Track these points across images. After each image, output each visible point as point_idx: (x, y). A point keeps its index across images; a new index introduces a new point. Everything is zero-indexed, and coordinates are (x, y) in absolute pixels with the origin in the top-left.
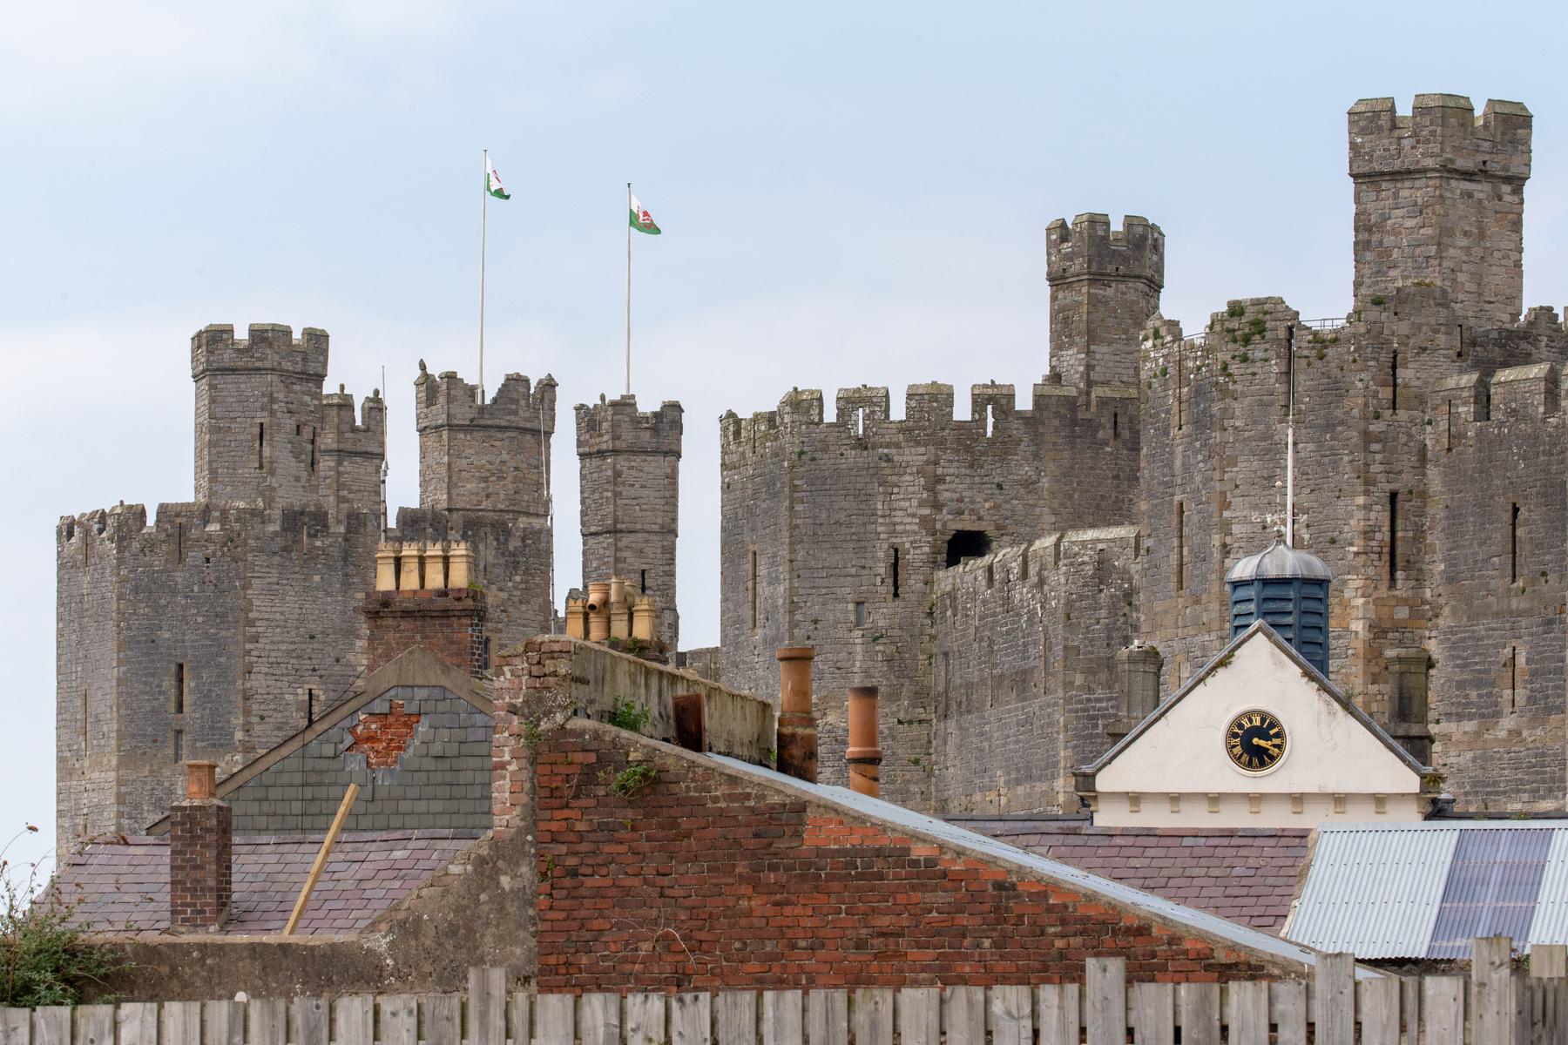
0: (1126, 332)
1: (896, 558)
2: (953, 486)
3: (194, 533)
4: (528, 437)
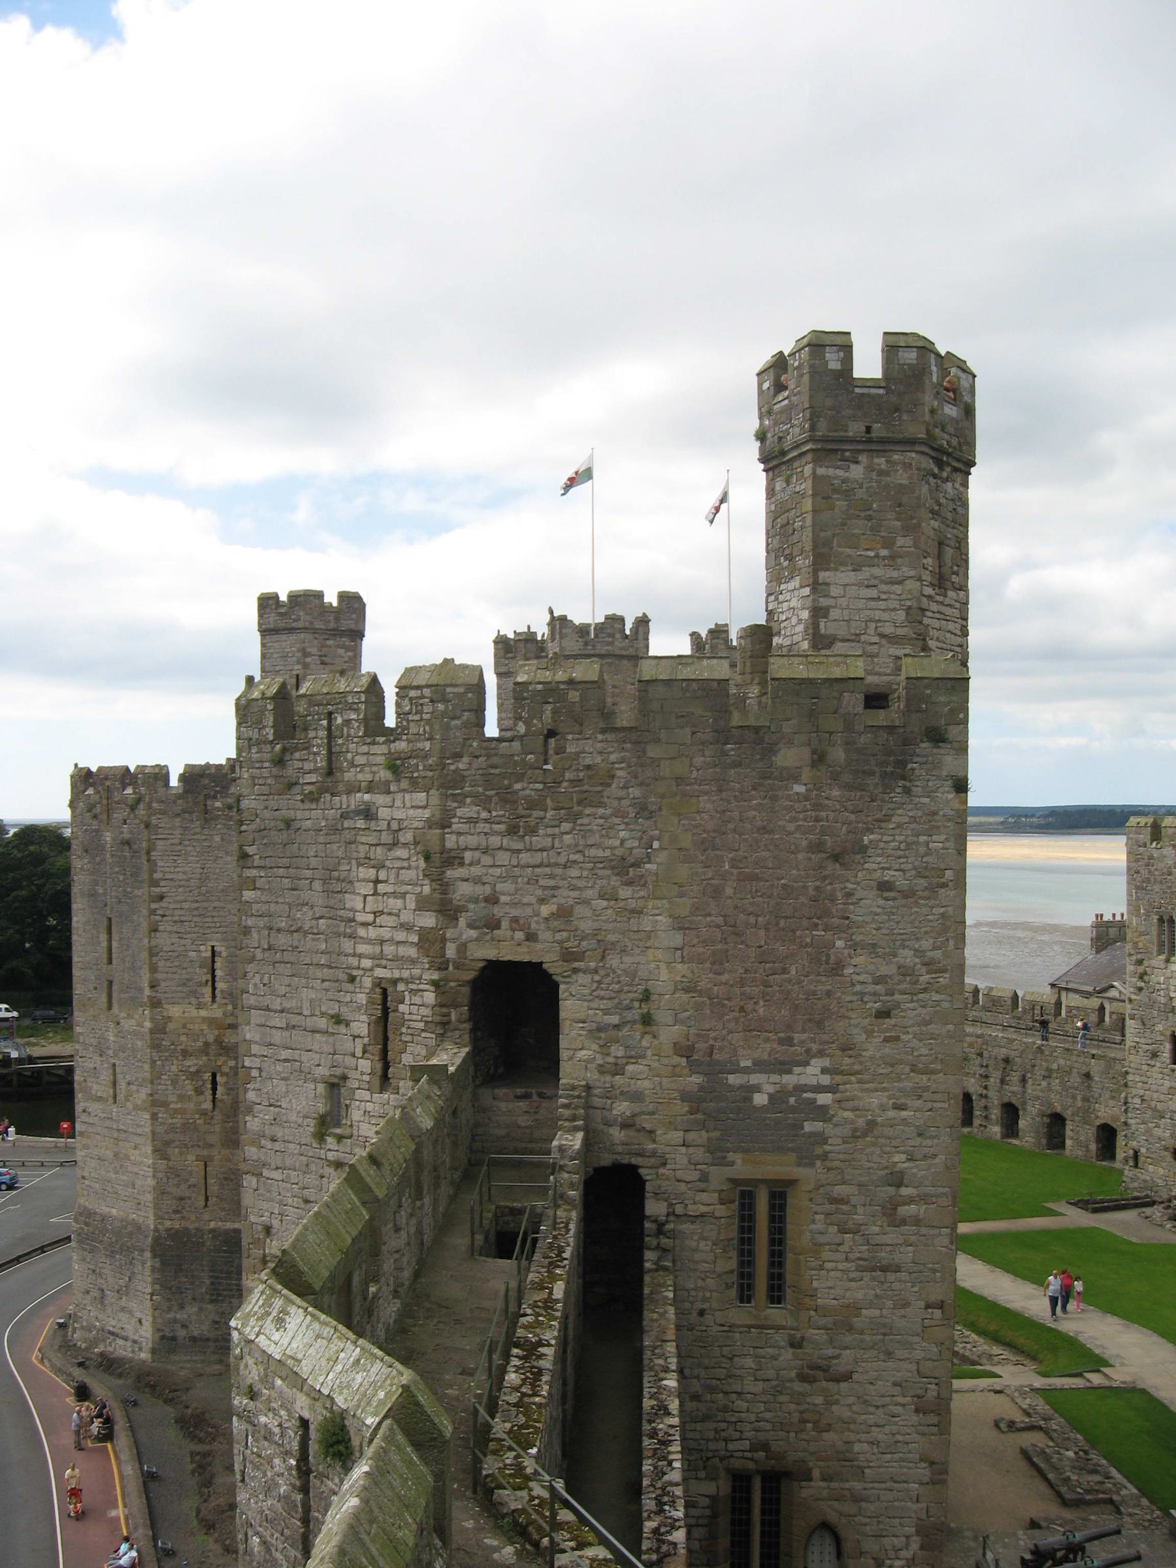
0: (888, 543)
1: (386, 1011)
2: (476, 871)
3: (117, 796)
4: (625, 662)
